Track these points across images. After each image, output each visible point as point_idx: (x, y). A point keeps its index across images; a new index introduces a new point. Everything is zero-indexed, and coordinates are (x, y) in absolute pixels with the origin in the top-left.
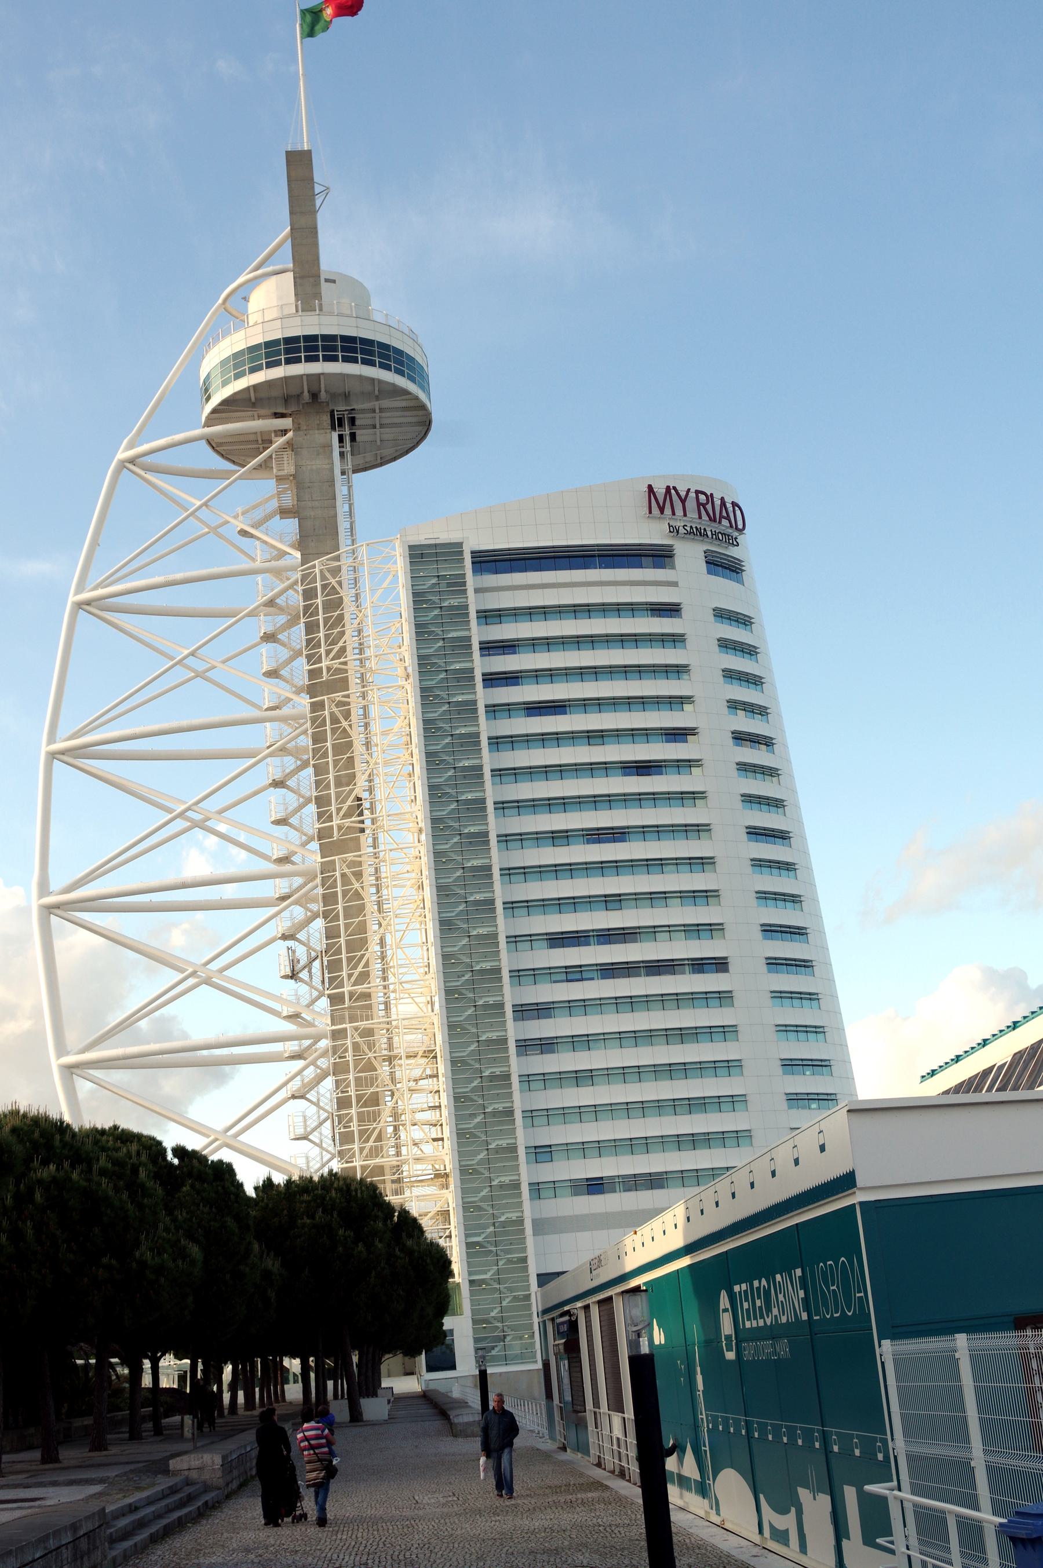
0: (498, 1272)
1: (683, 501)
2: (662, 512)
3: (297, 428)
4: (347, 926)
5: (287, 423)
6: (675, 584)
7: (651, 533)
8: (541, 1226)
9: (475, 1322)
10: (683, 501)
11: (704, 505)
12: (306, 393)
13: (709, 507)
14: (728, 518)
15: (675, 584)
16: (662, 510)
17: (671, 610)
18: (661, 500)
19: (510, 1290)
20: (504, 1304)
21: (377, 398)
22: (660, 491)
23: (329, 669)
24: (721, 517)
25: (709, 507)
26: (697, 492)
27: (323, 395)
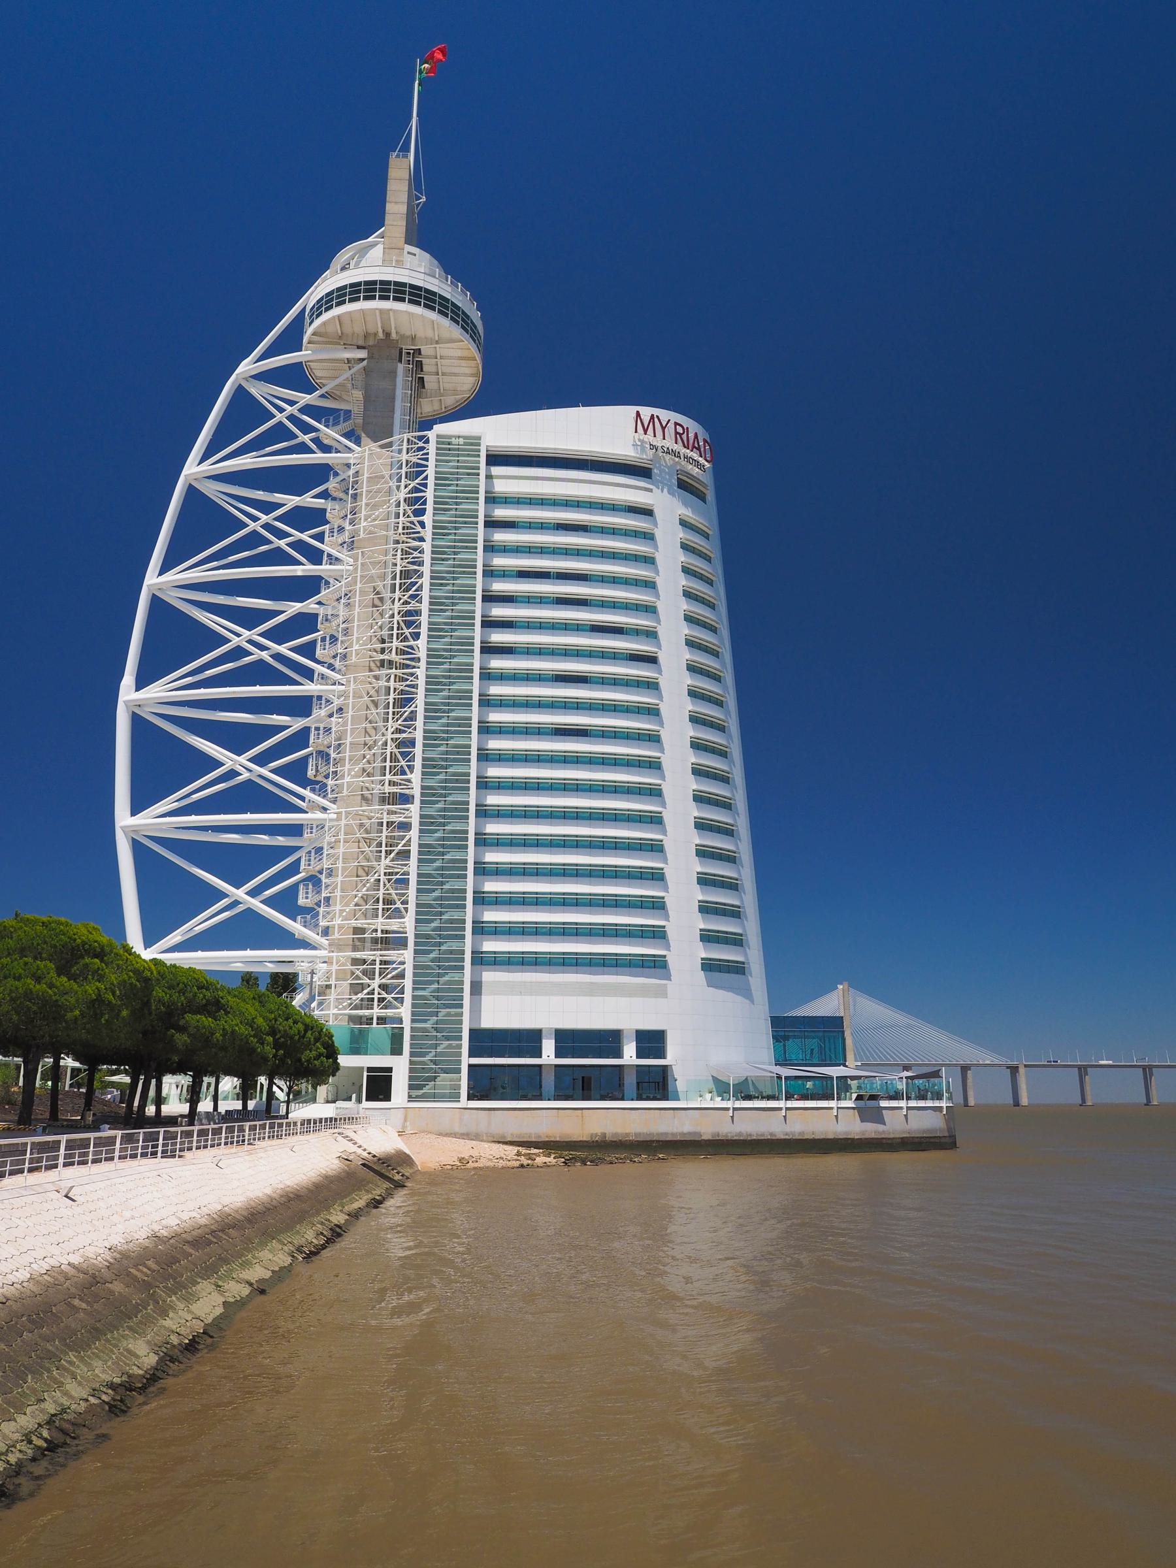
1: (663, 428)
2: (645, 432)
9: (411, 1062)
11: (681, 435)
12: (380, 331)
13: (684, 436)
14: (698, 449)
16: (645, 432)
21: (437, 342)
23: (365, 530)
24: (694, 447)
25: (684, 436)
26: (676, 424)
27: (394, 336)
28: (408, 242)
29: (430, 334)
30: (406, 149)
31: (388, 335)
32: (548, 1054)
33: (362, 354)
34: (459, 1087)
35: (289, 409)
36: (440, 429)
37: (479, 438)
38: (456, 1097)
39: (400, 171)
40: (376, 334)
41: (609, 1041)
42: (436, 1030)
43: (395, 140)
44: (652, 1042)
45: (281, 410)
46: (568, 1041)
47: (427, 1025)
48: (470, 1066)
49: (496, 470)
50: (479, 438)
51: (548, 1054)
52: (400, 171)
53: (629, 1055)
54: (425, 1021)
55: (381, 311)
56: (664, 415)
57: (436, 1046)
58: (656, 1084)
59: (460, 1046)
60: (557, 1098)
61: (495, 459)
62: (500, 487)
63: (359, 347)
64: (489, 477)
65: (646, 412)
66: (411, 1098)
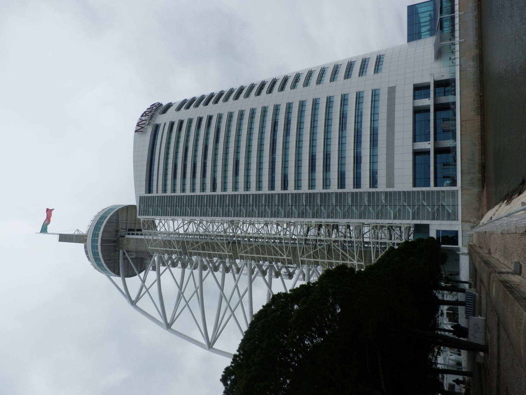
0: (409, 206)
1: (143, 121)
3: (122, 248)
4: (263, 254)
5: (121, 252)
6: (165, 123)
7: (150, 130)
8: (390, 182)
9: (433, 219)
10: (143, 121)
15: (165, 123)
16: (142, 128)
18: (140, 128)
19: (418, 200)
20: (425, 204)
21: (118, 221)
22: (139, 128)
27: (115, 239)
32: (429, 145)
34: (448, 192)
37: (140, 197)
38: (454, 194)
41: (419, 112)
42: (414, 206)
44: (420, 90)
47: (411, 210)
48: (436, 185)
50: (140, 197)
53: (428, 102)
54: (409, 212)
55: (101, 243)
57: (423, 205)
58: (444, 85)
59: (423, 192)
60: (454, 138)
61: (149, 189)
66: (456, 219)
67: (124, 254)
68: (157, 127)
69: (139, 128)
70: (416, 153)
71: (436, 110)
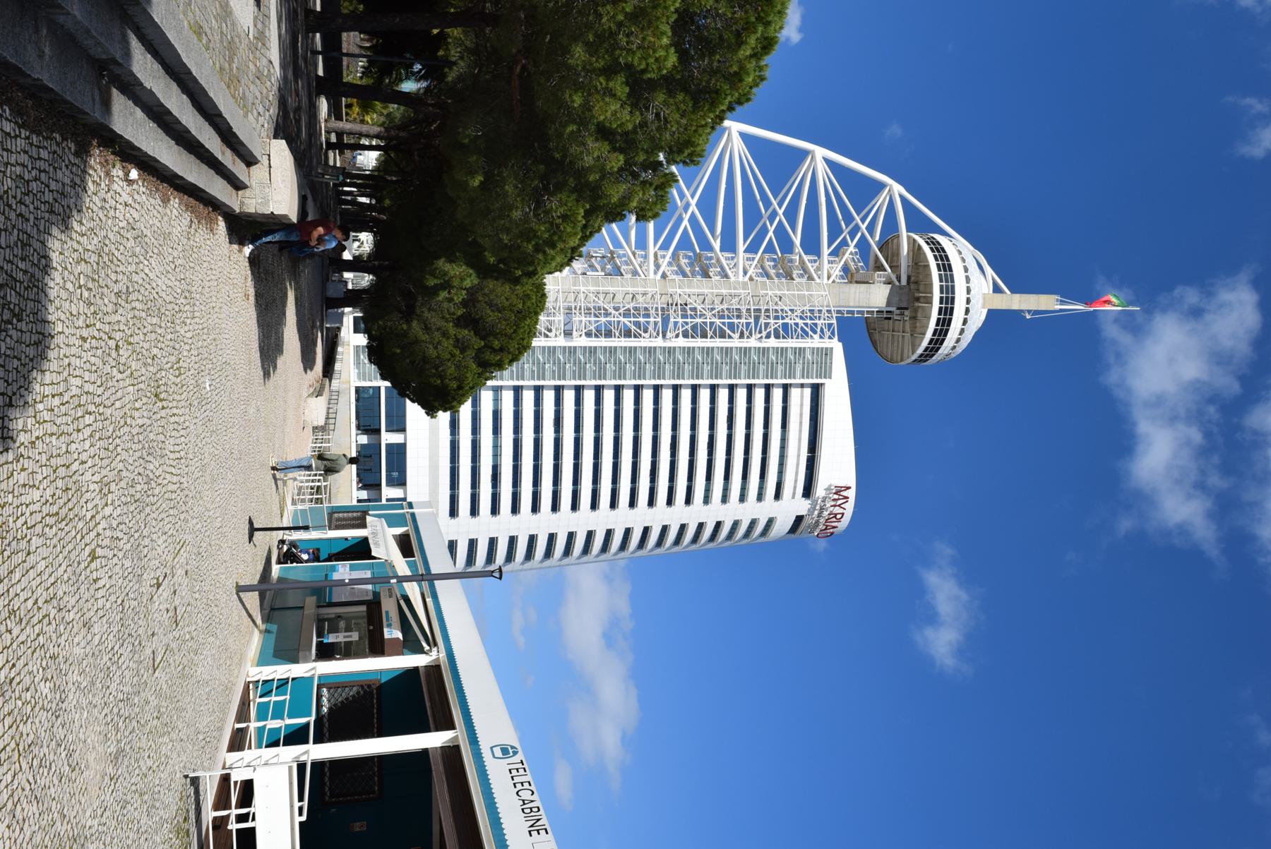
3: (901, 288)
17: (778, 496)
28: (990, 311)
29: (918, 330)
30: (1062, 302)
31: (918, 299)
33: (904, 282)
35: (863, 227)
36: (837, 348)
39: (1048, 303)
40: (918, 291)
43: (1067, 294)
45: (863, 220)
46: (398, 453)
49: (808, 391)
51: (388, 438)
52: (1048, 303)
56: (850, 507)
61: (816, 390)
62: (795, 393)
63: (909, 278)
64: (802, 386)
65: (851, 494)
67: (899, 279)
68: (808, 492)
69: (844, 493)
70: (402, 430)
71: (380, 485)
